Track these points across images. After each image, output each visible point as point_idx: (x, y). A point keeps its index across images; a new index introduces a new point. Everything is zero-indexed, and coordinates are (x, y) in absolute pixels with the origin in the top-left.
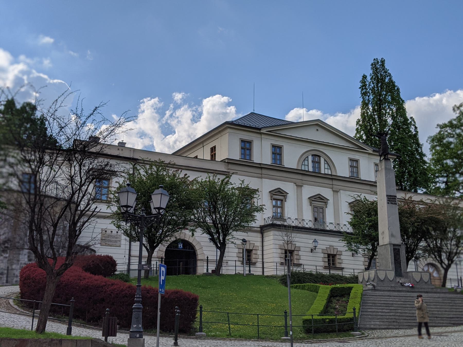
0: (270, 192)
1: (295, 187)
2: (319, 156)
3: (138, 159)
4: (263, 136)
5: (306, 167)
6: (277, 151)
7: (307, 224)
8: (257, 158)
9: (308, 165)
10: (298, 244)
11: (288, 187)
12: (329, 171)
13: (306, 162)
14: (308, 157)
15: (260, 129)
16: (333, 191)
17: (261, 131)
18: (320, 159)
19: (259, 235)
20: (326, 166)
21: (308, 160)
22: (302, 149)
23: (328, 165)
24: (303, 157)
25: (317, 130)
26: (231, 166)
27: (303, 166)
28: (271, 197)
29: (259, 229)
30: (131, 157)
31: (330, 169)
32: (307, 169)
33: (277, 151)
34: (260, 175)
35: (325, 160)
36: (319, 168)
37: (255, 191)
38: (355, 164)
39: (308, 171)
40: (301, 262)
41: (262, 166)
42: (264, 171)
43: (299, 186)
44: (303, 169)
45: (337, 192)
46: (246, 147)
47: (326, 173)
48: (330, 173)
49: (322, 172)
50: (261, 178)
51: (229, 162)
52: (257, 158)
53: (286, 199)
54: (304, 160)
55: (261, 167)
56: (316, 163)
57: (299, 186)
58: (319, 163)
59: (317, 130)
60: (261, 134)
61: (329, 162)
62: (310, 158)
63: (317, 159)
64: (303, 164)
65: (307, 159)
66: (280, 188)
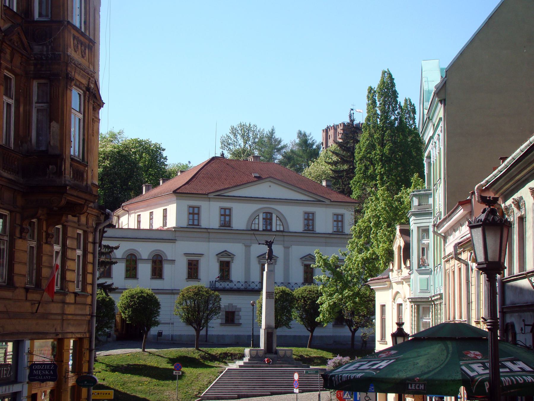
1: (244, 247)
4: (211, 199)
5: (257, 226)
6: (226, 214)
7: (249, 285)
8: (204, 223)
10: (239, 306)
11: (236, 248)
12: (282, 227)
13: (257, 221)
14: (259, 215)
15: (207, 195)
16: (285, 247)
20: (279, 222)
22: (254, 207)
23: (280, 220)
24: (254, 216)
25: (270, 186)
26: (178, 234)
27: (253, 225)
32: (257, 228)
33: (226, 214)
35: (277, 217)
36: (271, 224)
39: (258, 230)
40: (241, 321)
43: (248, 246)
44: (253, 228)
45: (289, 248)
46: (194, 213)
47: (278, 229)
48: (282, 229)
50: (209, 242)
51: (176, 230)
52: (204, 223)
53: (233, 260)
56: (268, 220)
57: (248, 246)
58: (271, 219)
59: (270, 186)
61: (281, 218)
62: (261, 216)
64: (254, 222)
65: (257, 217)
66: (226, 251)
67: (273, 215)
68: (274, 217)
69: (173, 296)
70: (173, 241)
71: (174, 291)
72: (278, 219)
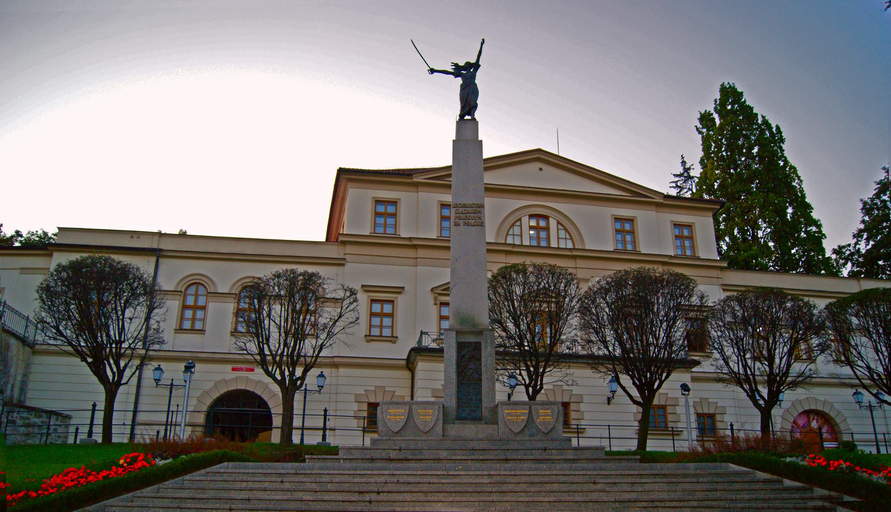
0: (432, 290)
2: (546, 218)
3: (161, 250)
4: (420, 188)
9: (521, 235)
13: (517, 230)
14: (520, 220)
17: (415, 180)
18: (548, 223)
19: (407, 374)
20: (562, 234)
21: (521, 226)
26: (349, 249)
28: (436, 299)
29: (404, 362)
30: (156, 247)
31: (571, 239)
32: (518, 242)
34: (413, 261)
35: (558, 223)
36: (548, 239)
37: (400, 290)
38: (627, 227)
39: (522, 246)
41: (414, 242)
42: (421, 253)
47: (562, 245)
48: (570, 246)
49: (554, 244)
54: (513, 225)
55: (412, 244)
58: (547, 229)
59: (541, 169)
60: (417, 185)
63: (542, 223)
64: (511, 232)
65: (518, 223)
67: (551, 219)
68: (553, 223)
69: (334, 370)
70: (340, 263)
71: (335, 360)
72: (560, 227)
